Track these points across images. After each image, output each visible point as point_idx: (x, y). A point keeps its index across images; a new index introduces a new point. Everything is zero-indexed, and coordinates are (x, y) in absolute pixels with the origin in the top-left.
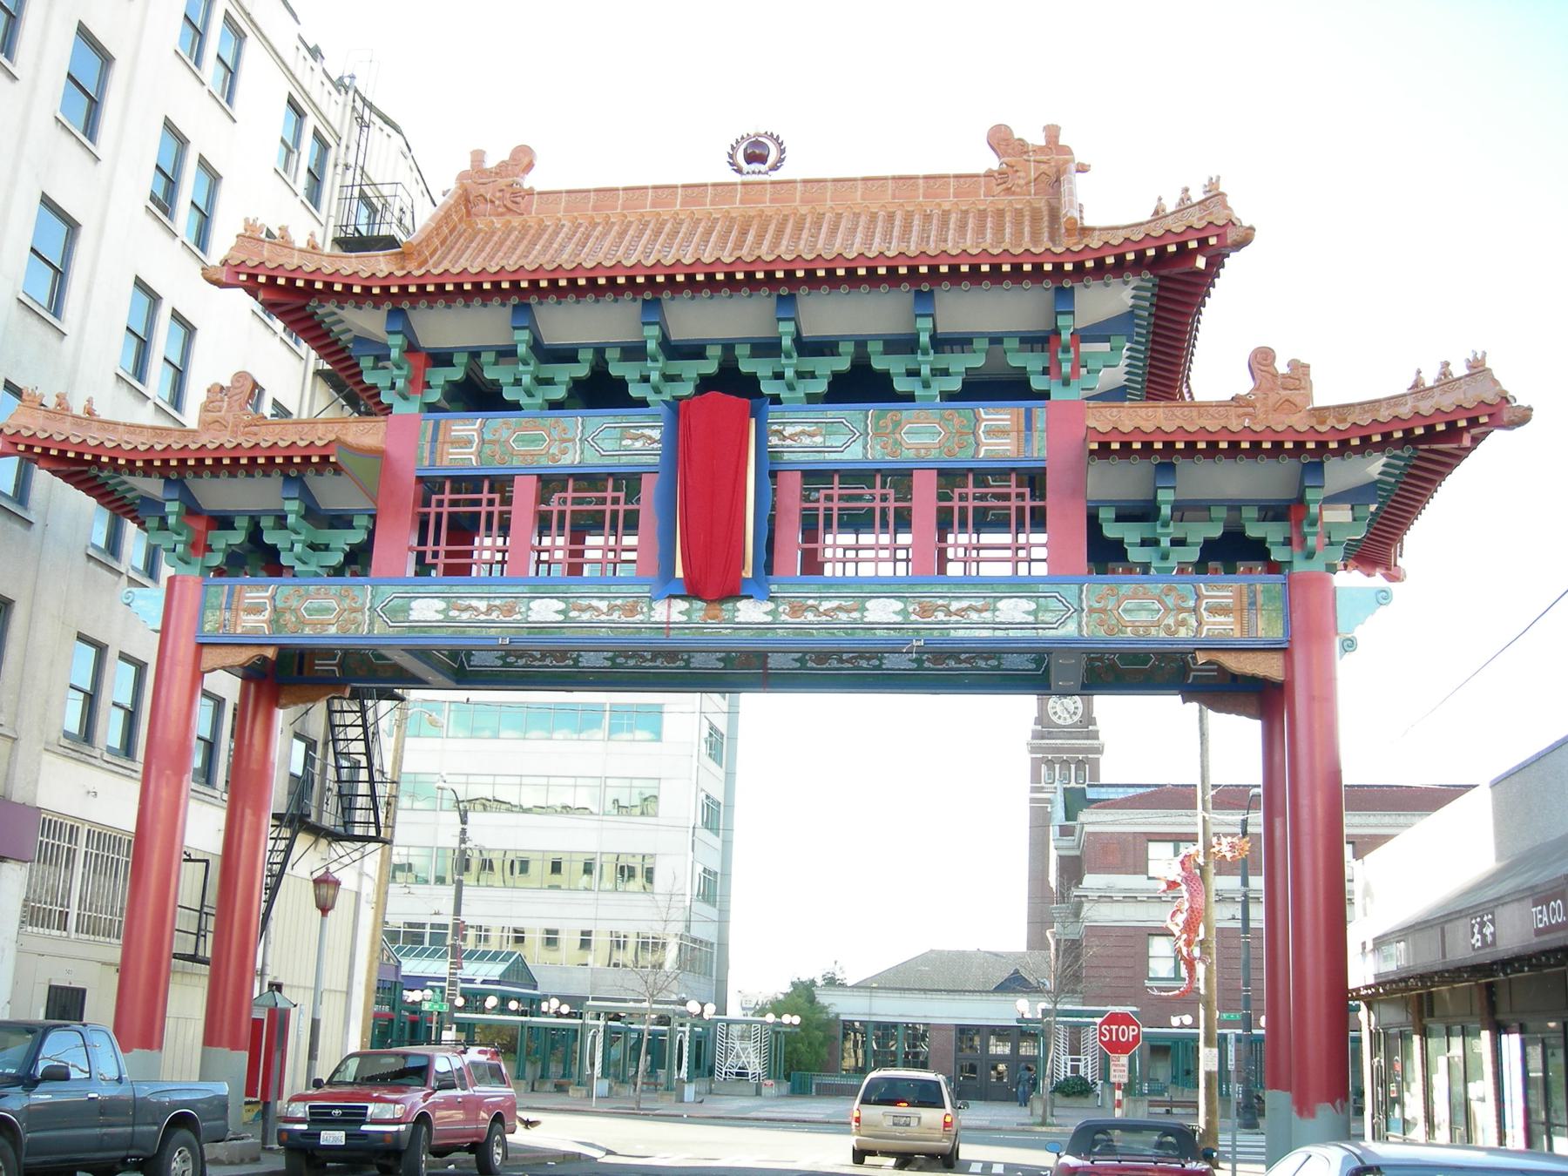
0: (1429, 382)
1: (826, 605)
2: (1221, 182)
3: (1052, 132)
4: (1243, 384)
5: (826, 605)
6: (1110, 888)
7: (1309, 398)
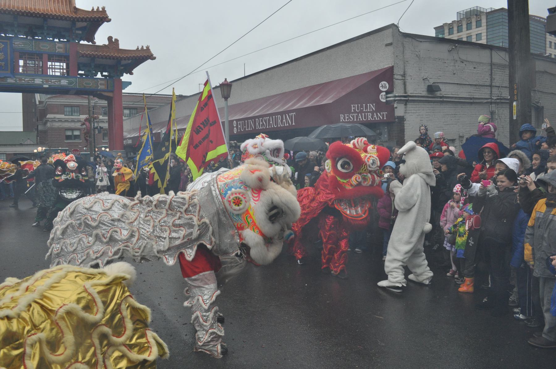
0: (140, 49)
1: (26, 80)
2: (106, 8)
4: (107, 43)
5: (26, 80)
6: (55, 118)
7: (119, 47)
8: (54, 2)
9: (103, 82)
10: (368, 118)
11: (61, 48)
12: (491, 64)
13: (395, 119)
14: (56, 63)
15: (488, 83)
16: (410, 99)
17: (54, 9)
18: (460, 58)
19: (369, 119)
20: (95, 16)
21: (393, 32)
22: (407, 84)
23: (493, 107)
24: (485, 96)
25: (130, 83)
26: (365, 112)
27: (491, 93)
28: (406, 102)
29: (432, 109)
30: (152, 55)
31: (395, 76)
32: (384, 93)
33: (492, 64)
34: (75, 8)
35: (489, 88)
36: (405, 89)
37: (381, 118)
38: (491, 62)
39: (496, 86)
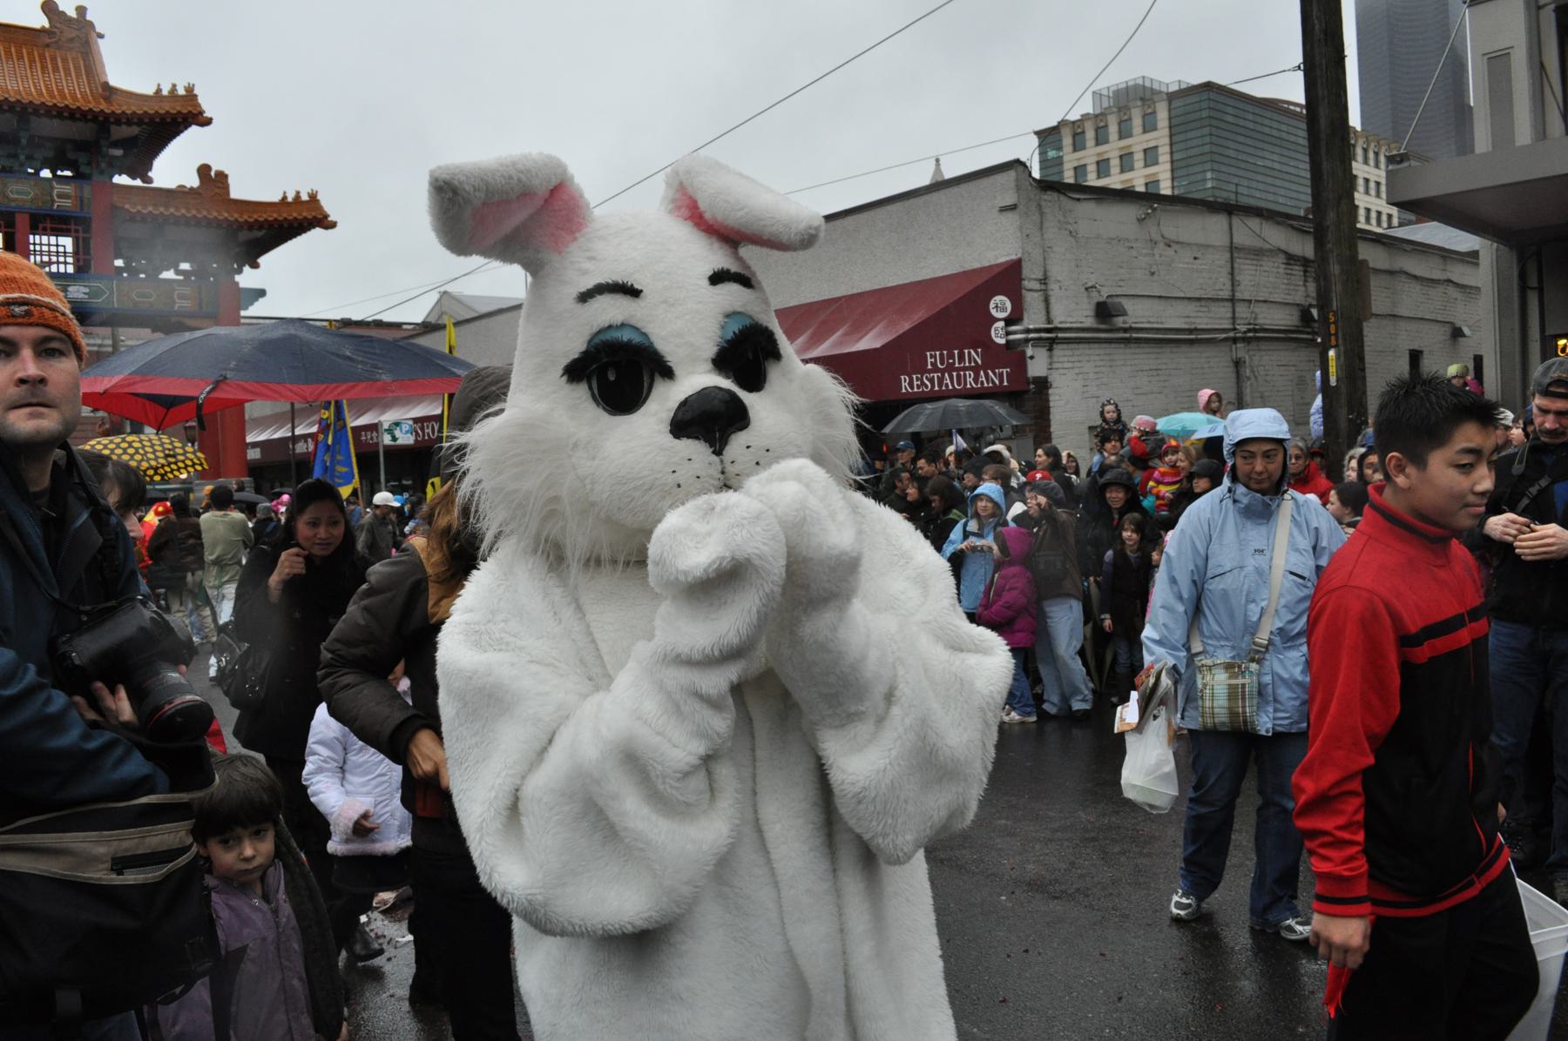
3: (81, 10)
4: (193, 181)
7: (228, 193)
8: (43, 73)
9: (187, 291)
10: (965, 384)
11: (66, 196)
12: (1231, 247)
13: (1029, 383)
14: (59, 238)
15: (1226, 294)
16: (1060, 335)
17: (46, 86)
18: (1163, 236)
19: (969, 386)
20: (167, 109)
21: (1017, 180)
22: (1053, 300)
23: (1241, 350)
24: (1220, 324)
25: (261, 293)
26: (958, 370)
27: (1234, 318)
28: (1051, 344)
29: (1107, 357)
30: (326, 216)
31: (1026, 283)
32: (1001, 324)
33: (1232, 248)
34: (106, 86)
35: (1229, 304)
36: (1048, 312)
37: (997, 382)
38: (1232, 243)
39: (1243, 300)
